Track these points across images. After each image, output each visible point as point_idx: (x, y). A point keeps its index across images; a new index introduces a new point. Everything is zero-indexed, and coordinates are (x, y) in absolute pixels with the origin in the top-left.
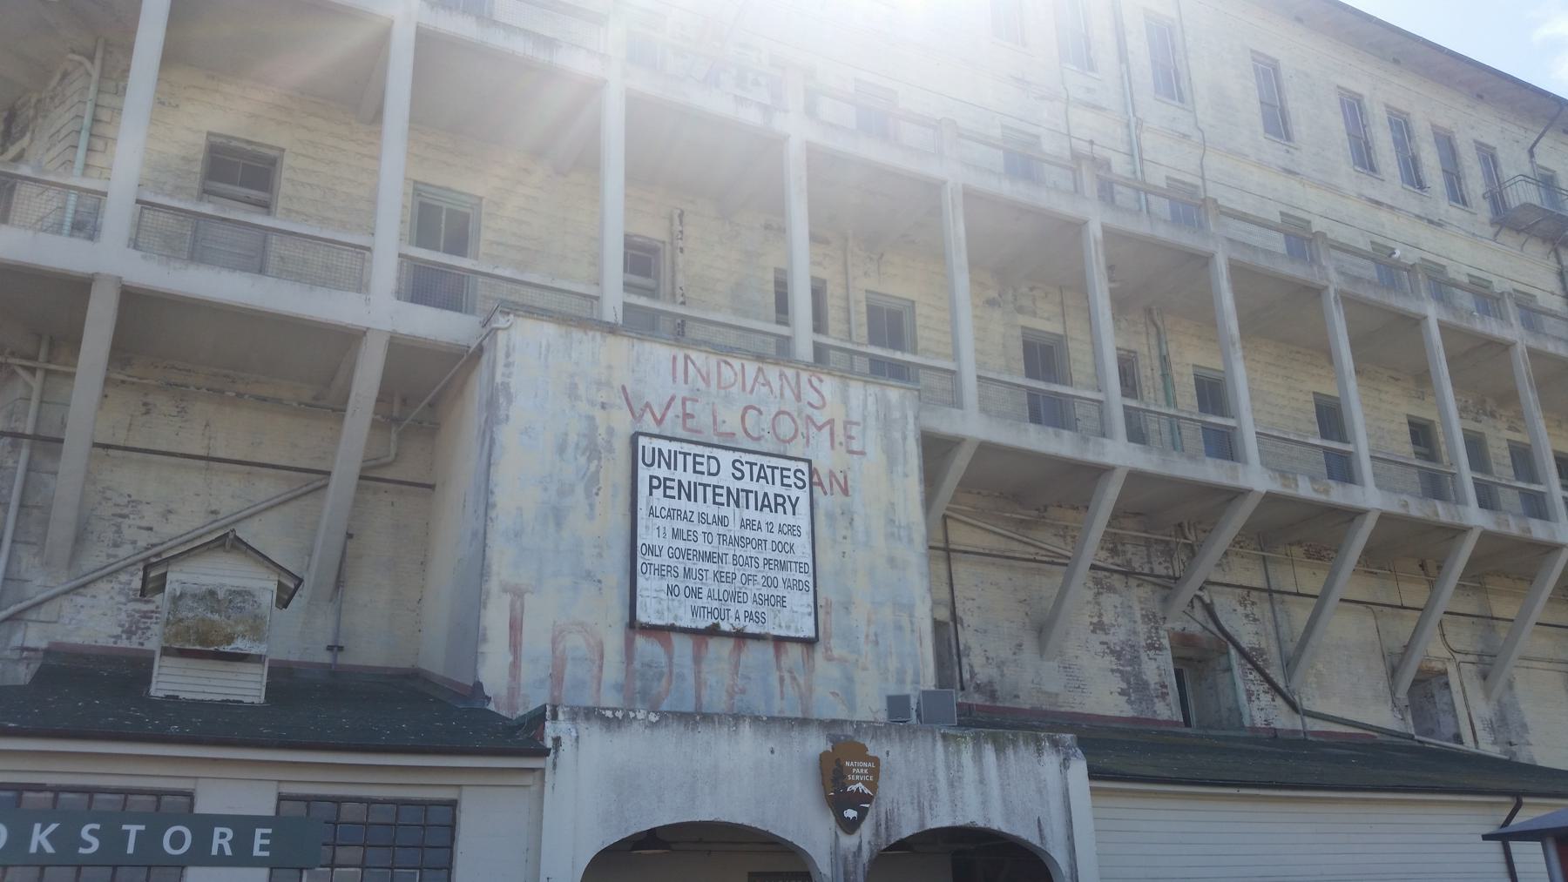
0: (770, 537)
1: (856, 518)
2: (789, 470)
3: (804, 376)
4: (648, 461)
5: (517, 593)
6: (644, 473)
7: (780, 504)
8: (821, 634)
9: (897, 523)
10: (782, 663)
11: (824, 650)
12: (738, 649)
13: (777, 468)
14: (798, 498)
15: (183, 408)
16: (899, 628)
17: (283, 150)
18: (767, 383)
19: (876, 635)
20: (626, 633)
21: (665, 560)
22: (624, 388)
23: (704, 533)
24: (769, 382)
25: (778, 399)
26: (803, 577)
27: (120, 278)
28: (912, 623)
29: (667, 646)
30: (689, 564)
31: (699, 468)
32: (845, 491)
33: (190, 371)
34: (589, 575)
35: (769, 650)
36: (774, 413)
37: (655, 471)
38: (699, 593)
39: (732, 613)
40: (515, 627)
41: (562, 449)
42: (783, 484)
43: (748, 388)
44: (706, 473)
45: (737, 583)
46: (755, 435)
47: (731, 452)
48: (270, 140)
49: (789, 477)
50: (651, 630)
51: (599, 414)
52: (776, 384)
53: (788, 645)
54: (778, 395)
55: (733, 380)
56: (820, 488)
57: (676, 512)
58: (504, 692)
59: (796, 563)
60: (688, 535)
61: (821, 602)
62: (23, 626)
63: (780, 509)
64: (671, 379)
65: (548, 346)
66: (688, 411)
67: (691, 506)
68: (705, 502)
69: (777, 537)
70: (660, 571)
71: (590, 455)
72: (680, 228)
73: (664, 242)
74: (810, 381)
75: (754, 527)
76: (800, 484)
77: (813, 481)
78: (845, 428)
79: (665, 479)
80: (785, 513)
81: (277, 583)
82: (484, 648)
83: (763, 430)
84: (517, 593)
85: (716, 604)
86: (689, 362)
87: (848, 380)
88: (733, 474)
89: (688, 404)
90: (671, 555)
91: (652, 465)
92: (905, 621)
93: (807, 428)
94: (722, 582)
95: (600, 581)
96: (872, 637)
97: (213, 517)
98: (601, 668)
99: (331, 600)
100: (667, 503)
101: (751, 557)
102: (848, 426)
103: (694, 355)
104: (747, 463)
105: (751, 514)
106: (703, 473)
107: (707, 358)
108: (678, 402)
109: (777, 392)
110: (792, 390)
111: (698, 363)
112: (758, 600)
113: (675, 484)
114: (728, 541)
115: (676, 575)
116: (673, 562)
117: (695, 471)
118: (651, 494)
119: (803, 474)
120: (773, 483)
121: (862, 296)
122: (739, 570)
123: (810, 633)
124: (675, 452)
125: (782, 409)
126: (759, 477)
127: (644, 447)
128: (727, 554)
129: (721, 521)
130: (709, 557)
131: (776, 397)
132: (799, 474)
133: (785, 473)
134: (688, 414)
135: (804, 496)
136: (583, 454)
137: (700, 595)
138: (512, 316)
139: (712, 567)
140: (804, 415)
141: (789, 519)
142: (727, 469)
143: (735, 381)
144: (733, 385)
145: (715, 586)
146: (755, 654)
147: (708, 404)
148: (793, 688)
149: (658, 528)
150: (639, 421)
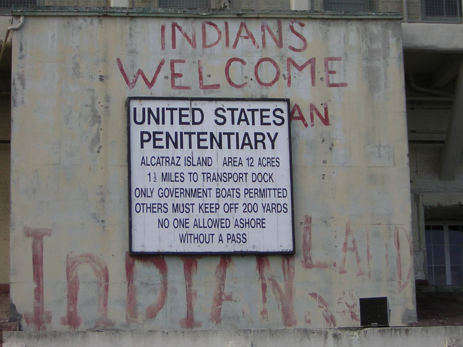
0: (250, 170)
2: (269, 110)
3: (285, 25)
4: (139, 120)
6: (136, 130)
7: (259, 141)
10: (265, 274)
11: (303, 259)
18: (250, 36)
19: (354, 242)
20: (126, 258)
21: (155, 199)
22: (118, 60)
23: (190, 173)
24: (252, 35)
26: (282, 201)
29: (163, 269)
31: (184, 120)
32: (326, 121)
35: (252, 264)
36: (257, 61)
37: (145, 127)
38: (186, 223)
39: (216, 238)
42: (262, 124)
43: (232, 42)
44: (191, 123)
45: (221, 210)
49: (268, 117)
54: (261, 45)
55: (217, 38)
57: (164, 159)
59: (275, 189)
60: (176, 177)
63: (260, 145)
67: (178, 152)
69: (257, 169)
70: (151, 208)
74: (292, 28)
75: (236, 164)
76: (279, 121)
78: (326, 65)
79: (155, 133)
83: (246, 77)
86: (176, 28)
88: (216, 121)
89: (176, 65)
90: (161, 195)
93: (289, 70)
94: (206, 212)
95: (103, 221)
96: (350, 245)
98: (107, 288)
101: (233, 189)
102: (330, 62)
103: (180, 23)
104: (228, 109)
105: (234, 152)
106: (188, 124)
109: (259, 41)
110: (275, 40)
111: (184, 29)
112: (239, 224)
113: (163, 136)
114: (211, 178)
115: (166, 210)
117: (181, 123)
118: (142, 147)
119: (282, 112)
120: (253, 124)
124: (163, 109)
126: (240, 120)
128: (210, 189)
129: (205, 162)
131: (258, 47)
132: (278, 113)
133: (265, 113)
134: (177, 74)
135: (283, 131)
137: (187, 225)
138: (22, 19)
139: (197, 201)
140: (285, 59)
141: (269, 153)
143: (220, 38)
144: (217, 42)
147: (194, 62)
148: (275, 293)
149: (149, 174)
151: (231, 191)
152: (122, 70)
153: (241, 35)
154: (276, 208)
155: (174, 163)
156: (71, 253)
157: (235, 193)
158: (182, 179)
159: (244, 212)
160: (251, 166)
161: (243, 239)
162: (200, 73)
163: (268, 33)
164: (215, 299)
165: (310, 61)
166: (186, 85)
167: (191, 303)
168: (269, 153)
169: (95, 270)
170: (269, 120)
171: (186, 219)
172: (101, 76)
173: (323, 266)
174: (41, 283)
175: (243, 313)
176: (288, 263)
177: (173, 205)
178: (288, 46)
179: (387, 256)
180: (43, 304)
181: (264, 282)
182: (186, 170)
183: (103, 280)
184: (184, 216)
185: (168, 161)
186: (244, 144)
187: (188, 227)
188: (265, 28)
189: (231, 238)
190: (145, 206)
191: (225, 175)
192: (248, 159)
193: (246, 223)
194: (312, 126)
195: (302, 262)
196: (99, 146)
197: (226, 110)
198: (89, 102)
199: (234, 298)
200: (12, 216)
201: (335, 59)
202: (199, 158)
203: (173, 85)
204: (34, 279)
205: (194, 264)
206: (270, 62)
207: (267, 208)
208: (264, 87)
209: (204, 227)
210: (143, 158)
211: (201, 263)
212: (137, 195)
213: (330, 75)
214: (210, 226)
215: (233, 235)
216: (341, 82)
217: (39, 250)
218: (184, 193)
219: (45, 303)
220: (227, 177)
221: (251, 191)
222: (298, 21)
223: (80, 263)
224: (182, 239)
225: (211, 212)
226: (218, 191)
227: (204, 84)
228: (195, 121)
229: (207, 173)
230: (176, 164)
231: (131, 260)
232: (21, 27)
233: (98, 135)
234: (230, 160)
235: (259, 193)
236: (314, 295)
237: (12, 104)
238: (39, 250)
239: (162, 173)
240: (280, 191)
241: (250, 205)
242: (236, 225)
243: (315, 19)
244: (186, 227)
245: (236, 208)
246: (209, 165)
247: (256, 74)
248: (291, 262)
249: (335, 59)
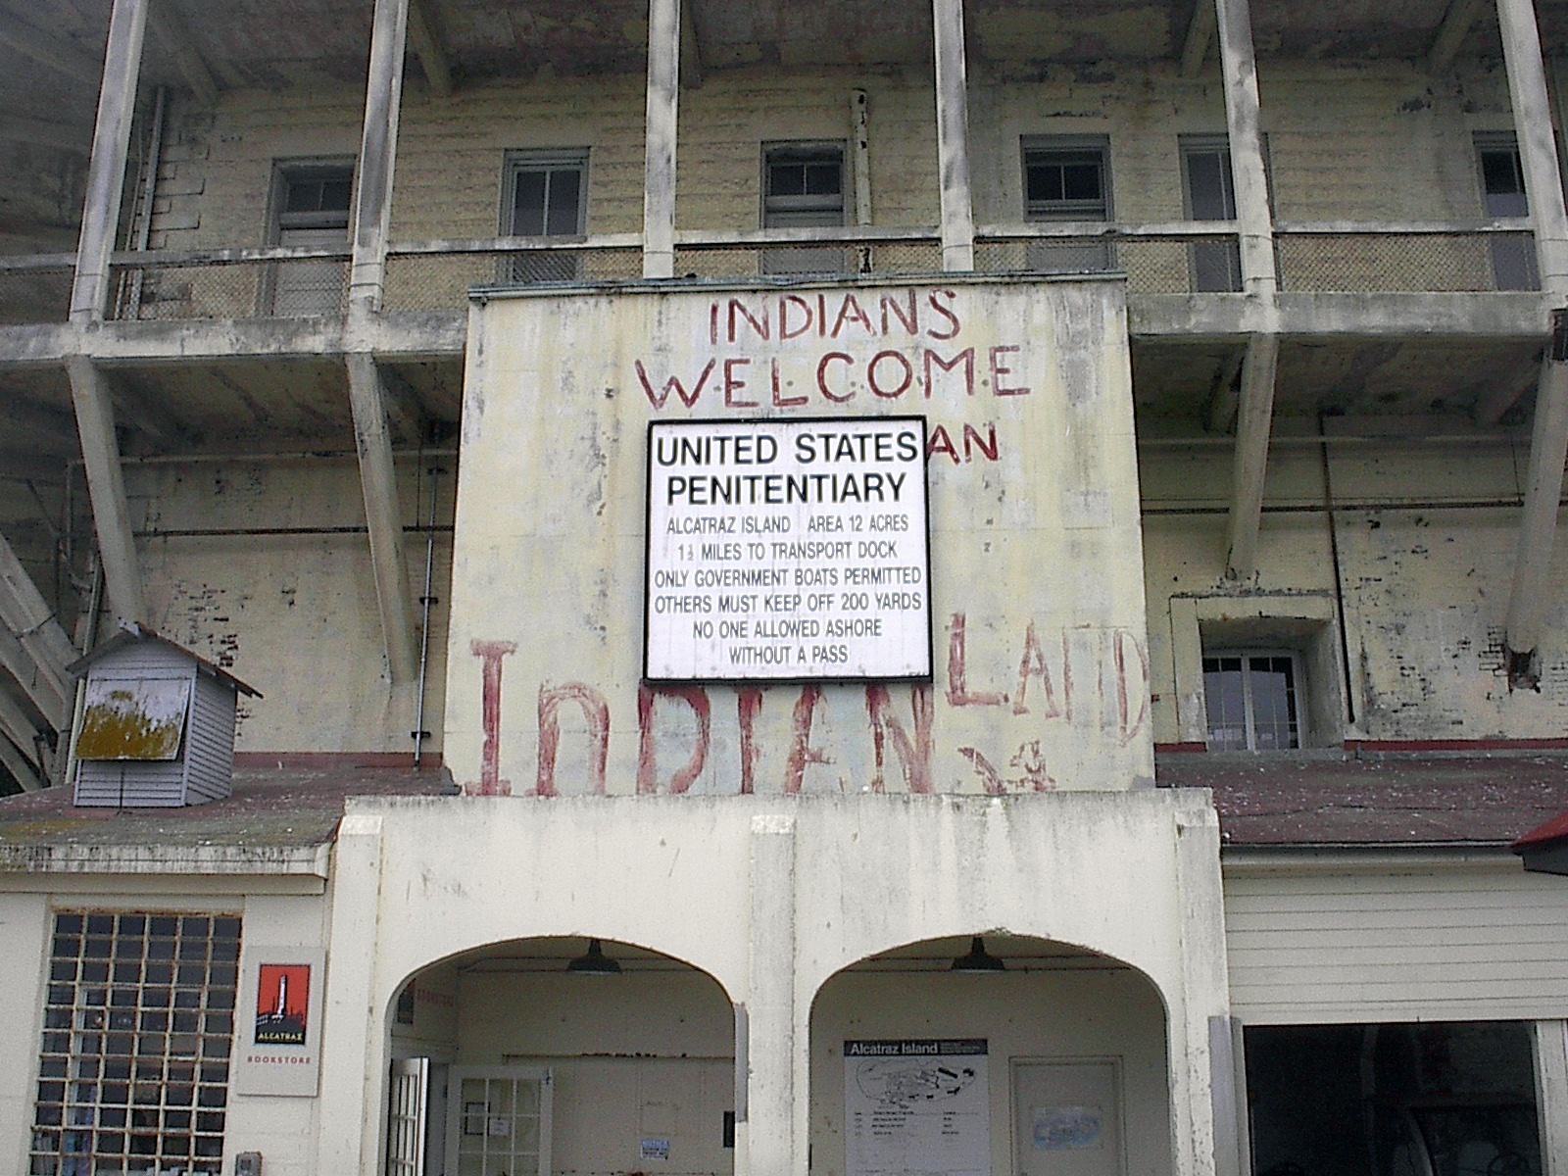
0: (856, 538)
1: (1007, 489)
2: (888, 435)
3: (923, 297)
4: (667, 456)
5: (492, 655)
6: (660, 475)
11: (949, 690)
14: (902, 477)
19: (1040, 658)
21: (690, 589)
22: (638, 363)
23: (751, 545)
26: (911, 589)
29: (702, 708)
30: (727, 592)
31: (743, 455)
32: (992, 453)
35: (859, 700)
37: (677, 470)
38: (742, 629)
40: (491, 697)
43: (830, 328)
45: (803, 607)
47: (796, 425)
49: (887, 446)
50: (671, 687)
56: (948, 454)
58: (477, 779)
59: (898, 569)
60: (727, 551)
61: (944, 619)
63: (873, 494)
68: (753, 499)
69: (868, 535)
70: (683, 604)
73: (845, 140)
74: (933, 301)
75: (830, 527)
76: (908, 453)
78: (993, 359)
79: (692, 479)
80: (881, 498)
83: (853, 384)
85: (768, 642)
86: (736, 309)
88: (799, 458)
90: (700, 582)
92: (1093, 635)
93: (927, 369)
94: (777, 610)
95: (603, 628)
98: (605, 740)
101: (825, 571)
102: (998, 354)
103: (742, 299)
104: (820, 436)
106: (748, 462)
108: (719, 368)
109: (877, 324)
110: (904, 320)
111: (749, 310)
113: (708, 484)
115: (707, 608)
117: (738, 461)
118: (671, 501)
119: (912, 436)
122: (804, 590)
126: (840, 453)
128: (785, 571)
129: (775, 525)
130: (757, 578)
131: (875, 333)
132: (906, 440)
133: (882, 441)
135: (914, 470)
137: (744, 632)
139: (762, 591)
140: (922, 352)
142: (788, 449)
144: (806, 327)
149: (681, 548)
150: (661, 405)
151: (822, 573)
152: (643, 379)
156: (547, 681)
157: (829, 577)
159: (844, 608)
160: (858, 529)
161: (841, 654)
162: (775, 379)
163: (892, 310)
164: (791, 759)
165: (964, 354)
166: (750, 400)
167: (749, 768)
168: (889, 506)
169: (587, 713)
171: (742, 623)
172: (609, 391)
175: (841, 784)
176: (922, 697)
177: (721, 600)
182: (743, 539)
184: (740, 616)
185: (714, 526)
186: (845, 493)
190: (673, 601)
192: (852, 519)
193: (847, 628)
194: (968, 461)
197: (815, 437)
198: (588, 433)
199: (824, 757)
201: (1008, 349)
203: (728, 401)
204: (485, 727)
207: (885, 602)
208: (884, 398)
212: (660, 582)
213: (999, 375)
214: (784, 632)
216: (1020, 385)
220: (815, 549)
222: (944, 289)
224: (735, 657)
225: (786, 609)
227: (781, 397)
228: (763, 457)
231: (647, 695)
234: (821, 521)
236: (968, 752)
241: (854, 598)
242: (829, 632)
244: (742, 636)
245: (829, 602)
246: (784, 531)
247: (871, 378)
248: (927, 694)
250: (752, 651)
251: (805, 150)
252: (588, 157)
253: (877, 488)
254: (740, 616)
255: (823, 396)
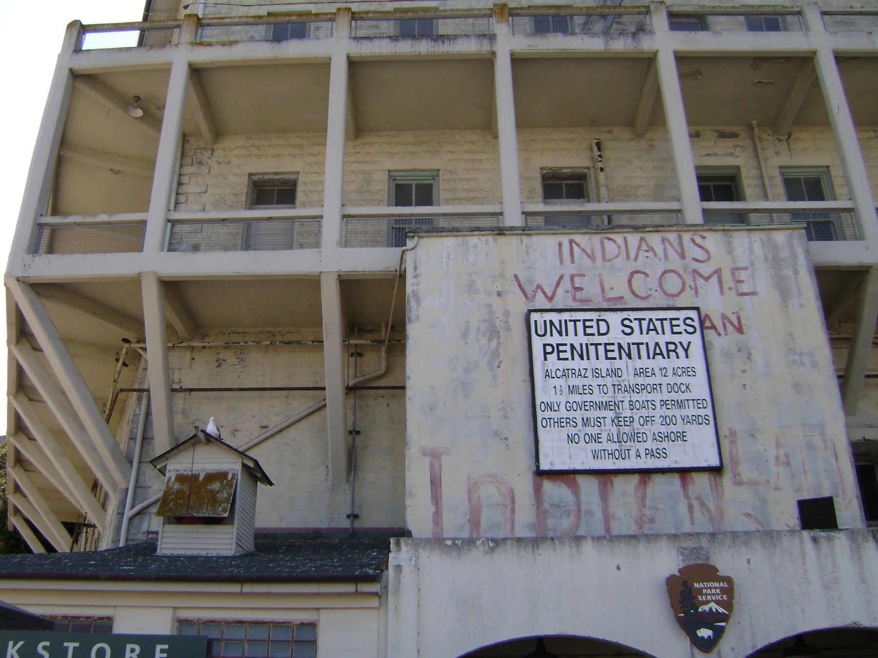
0: (664, 381)
1: (753, 351)
2: (678, 319)
3: (686, 237)
4: (541, 332)
5: (435, 456)
6: (537, 343)
8: (726, 461)
9: (798, 351)
11: (731, 475)
12: (643, 483)
13: (666, 319)
14: (689, 343)
15: (242, 359)
16: (811, 446)
17: (298, 173)
18: (651, 249)
19: (786, 456)
21: (563, 413)
22: (516, 277)
23: (599, 385)
25: (663, 260)
26: (702, 412)
27: (156, 272)
28: (824, 440)
30: (587, 415)
31: (588, 331)
32: (740, 330)
33: (245, 333)
34: (497, 434)
36: (660, 273)
37: (548, 339)
38: (598, 438)
39: (633, 453)
40: (435, 483)
41: (465, 334)
43: (632, 256)
44: (596, 334)
45: (636, 424)
46: (644, 295)
48: (289, 169)
49: (678, 326)
51: (495, 301)
52: (659, 249)
53: (695, 476)
55: (616, 253)
60: (584, 389)
61: (723, 432)
62: (148, 518)
63: (672, 354)
64: (558, 261)
65: (449, 254)
66: (577, 285)
67: (585, 364)
69: (671, 379)
70: (559, 423)
71: (490, 336)
72: (599, 153)
73: (588, 168)
74: (693, 240)
75: (648, 374)
76: (691, 330)
77: (704, 324)
78: (733, 274)
79: (558, 345)
80: (678, 357)
81: (241, 464)
82: (408, 502)
83: (650, 289)
84: (435, 456)
85: (615, 446)
86: (573, 244)
87: (731, 233)
88: (623, 331)
89: (576, 279)
90: (569, 409)
91: (545, 335)
93: (694, 280)
95: (506, 439)
96: (783, 459)
97: (264, 430)
99: (347, 482)
100: (561, 365)
101: (647, 401)
102: (736, 272)
103: (577, 238)
104: (635, 319)
105: (645, 362)
106: (593, 335)
107: (590, 239)
108: (567, 279)
109: (660, 253)
110: (676, 251)
111: (582, 245)
112: (658, 438)
113: (568, 348)
115: (575, 425)
116: (572, 414)
117: (586, 334)
118: (545, 359)
119: (693, 320)
121: (776, 173)
123: (714, 462)
124: (566, 321)
125: (668, 268)
126: (649, 330)
127: (536, 321)
129: (615, 373)
130: (606, 406)
131: (660, 259)
132: (689, 322)
134: (577, 288)
135: (696, 339)
136: (484, 335)
138: (416, 239)
139: (610, 415)
140: (690, 270)
141: (682, 362)
143: (619, 252)
144: (617, 256)
145: (614, 430)
146: (659, 486)
147: (595, 276)
148: (703, 513)
149: (555, 387)
153: (641, 249)
154: (697, 420)
155: (581, 375)
157: (650, 406)
158: (591, 392)
168: (682, 362)
170: (681, 329)
171: (598, 434)
173: (753, 483)
174: (440, 507)
177: (583, 418)
178: (691, 258)
179: (825, 470)
180: (442, 529)
181: (690, 502)
183: (509, 502)
184: (596, 430)
186: (655, 354)
187: (601, 442)
188: (665, 241)
189: (650, 453)
190: (552, 420)
191: (637, 386)
192: (661, 369)
194: (726, 335)
195: (731, 478)
196: (499, 360)
197: (633, 320)
200: (408, 434)
201: (742, 269)
202: (608, 369)
203: (574, 299)
204: (432, 502)
205: (609, 484)
206: (674, 274)
207: (686, 420)
209: (619, 442)
210: (547, 370)
211: (619, 482)
213: (738, 284)
215: (652, 450)
217: (438, 470)
218: (594, 406)
219: (444, 527)
220: (640, 388)
221: (667, 402)
223: (482, 484)
225: (625, 425)
226: (631, 403)
229: (618, 385)
230: (583, 376)
231: (539, 479)
232: (416, 246)
233: (498, 348)
235: (676, 405)
236: (748, 515)
237: (407, 321)
238: (438, 470)
239: (569, 386)
240: (699, 402)
241: (667, 418)
243: (716, 231)
244: (599, 442)
247: (661, 286)
249: (742, 269)
250: (606, 452)
251: (564, 173)
252: (437, 176)
253: (674, 351)
254: (596, 430)
255: (632, 296)
